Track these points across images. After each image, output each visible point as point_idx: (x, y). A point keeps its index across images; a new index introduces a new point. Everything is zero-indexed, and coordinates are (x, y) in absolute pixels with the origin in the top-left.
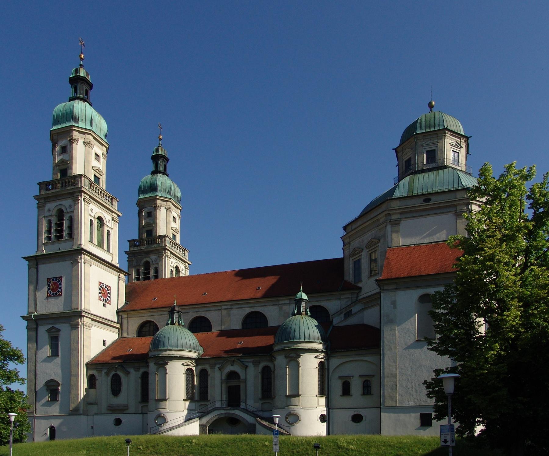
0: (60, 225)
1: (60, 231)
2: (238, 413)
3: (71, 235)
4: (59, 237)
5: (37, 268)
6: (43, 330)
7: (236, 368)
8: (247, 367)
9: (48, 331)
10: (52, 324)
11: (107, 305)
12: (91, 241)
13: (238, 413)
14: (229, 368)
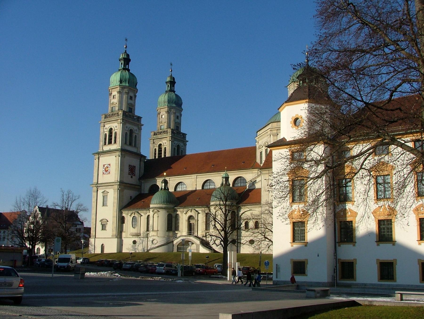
0: (110, 136)
1: (110, 140)
2: (192, 238)
3: (115, 142)
4: (110, 143)
5: (99, 159)
6: (100, 191)
7: (193, 213)
8: (199, 213)
9: (103, 192)
10: (105, 189)
11: (133, 177)
12: (126, 143)
13: (192, 238)
14: (189, 214)
